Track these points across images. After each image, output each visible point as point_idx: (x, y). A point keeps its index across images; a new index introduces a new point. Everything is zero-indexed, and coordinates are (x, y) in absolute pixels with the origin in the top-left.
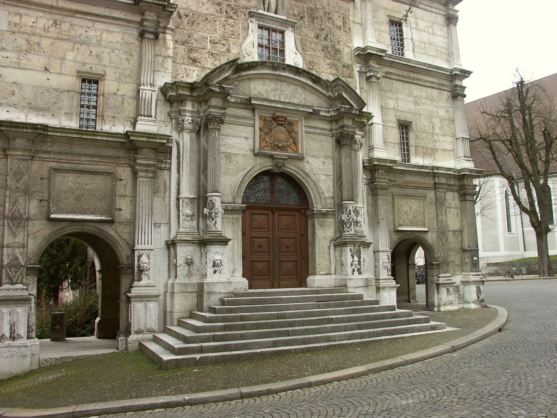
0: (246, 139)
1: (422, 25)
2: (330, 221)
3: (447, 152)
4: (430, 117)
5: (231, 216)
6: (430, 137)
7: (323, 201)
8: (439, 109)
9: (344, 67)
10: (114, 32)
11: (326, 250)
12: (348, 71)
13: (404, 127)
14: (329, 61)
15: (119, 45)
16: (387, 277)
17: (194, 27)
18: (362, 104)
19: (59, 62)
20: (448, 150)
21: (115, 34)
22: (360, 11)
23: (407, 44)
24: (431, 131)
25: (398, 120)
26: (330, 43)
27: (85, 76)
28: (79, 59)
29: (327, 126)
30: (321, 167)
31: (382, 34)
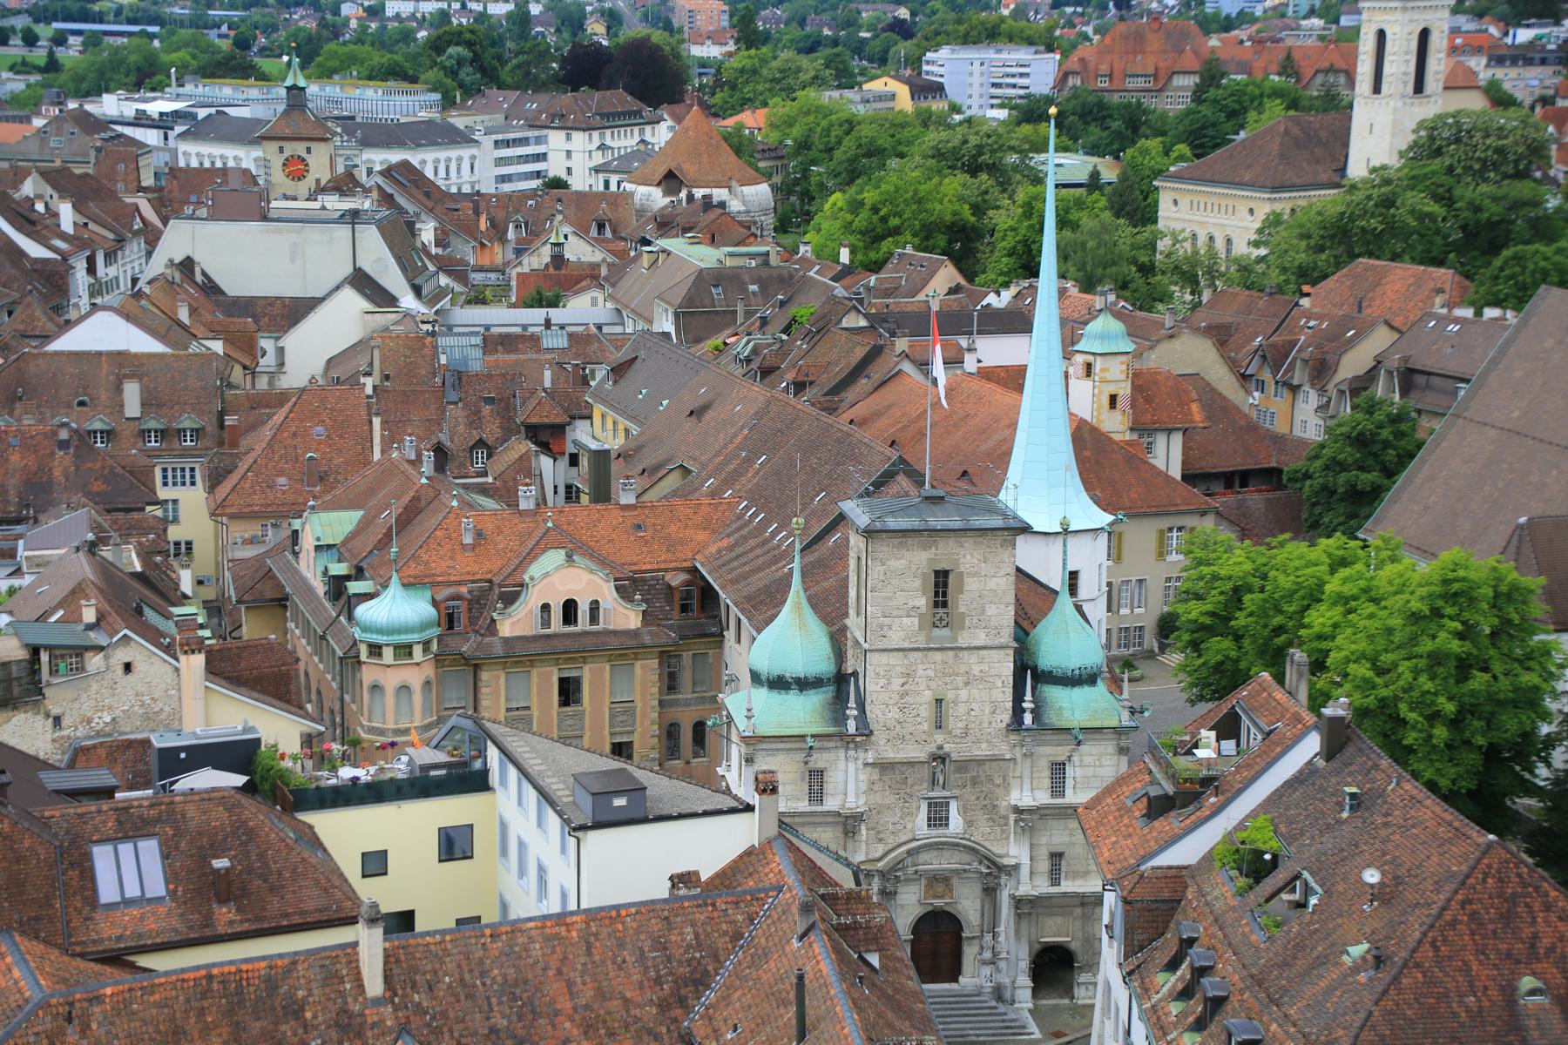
1: (1087, 760)
2: (976, 942)
13: (1056, 857)
23: (1069, 783)
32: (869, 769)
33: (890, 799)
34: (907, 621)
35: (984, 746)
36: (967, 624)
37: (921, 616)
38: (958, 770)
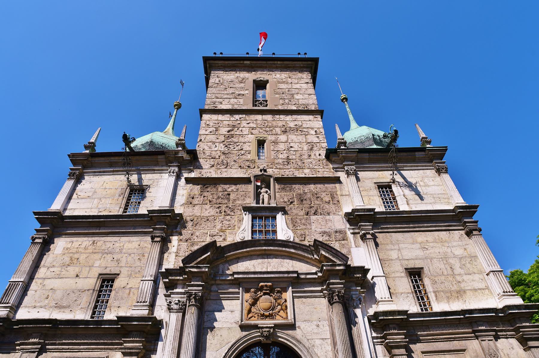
3: (479, 291)
4: (445, 258)
6: (451, 279)
8: (454, 250)
12: (341, 235)
13: (415, 274)
15: (136, 250)
17: (197, 227)
18: (344, 258)
20: (480, 289)
21: (134, 243)
22: (346, 185)
24: (450, 272)
25: (406, 269)
31: (372, 198)
33: (209, 211)
35: (307, 171)
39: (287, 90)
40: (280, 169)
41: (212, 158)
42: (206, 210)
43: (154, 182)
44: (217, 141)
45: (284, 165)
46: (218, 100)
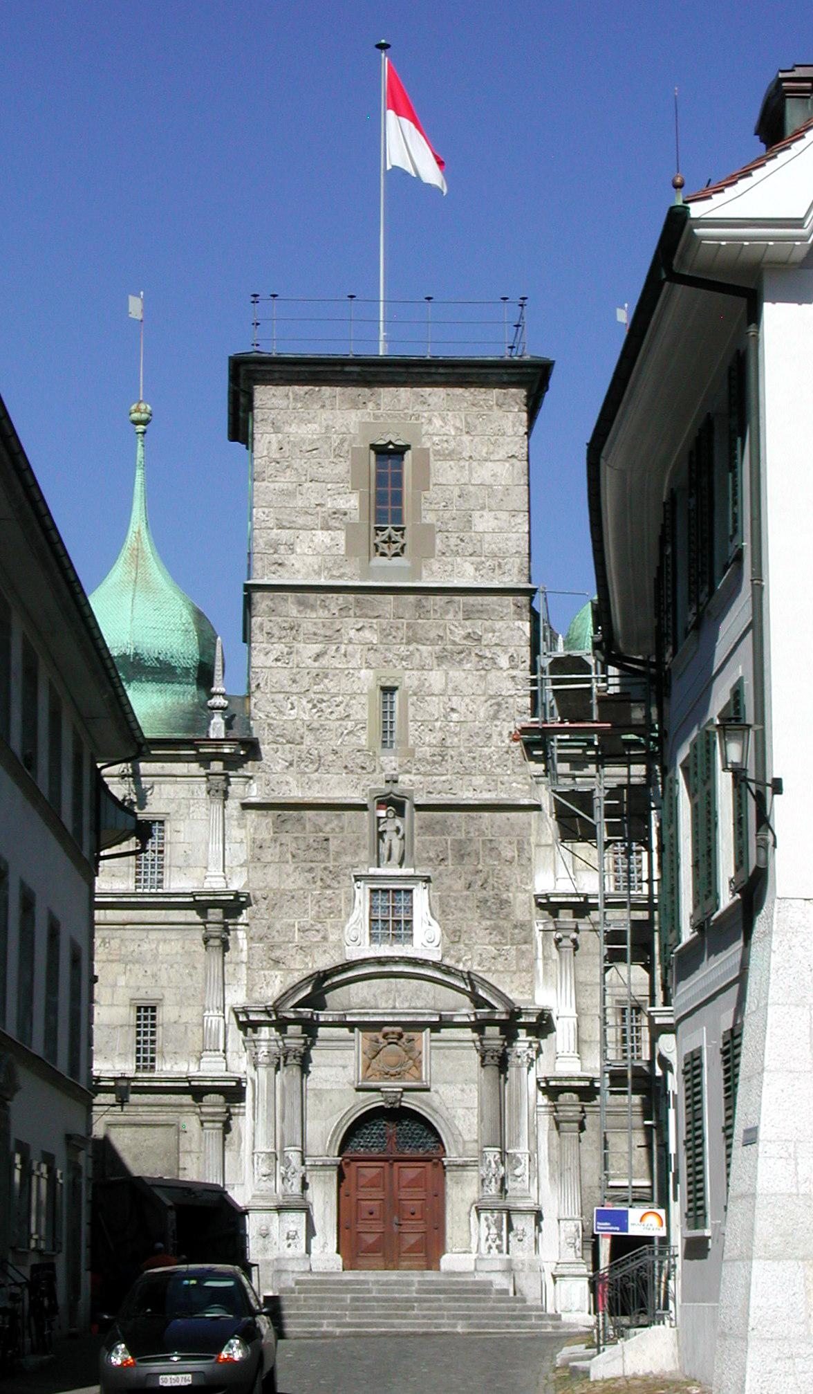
0: (344, 1067)
2: (472, 1175)
5: (321, 1173)
7: (460, 1147)
9: (515, 927)
10: (171, 940)
11: (464, 1217)
12: (523, 933)
14: (488, 923)
16: (573, 1259)
19: (109, 990)
26: (491, 893)
27: (140, 1003)
28: (132, 983)
29: (468, 1034)
30: (459, 1097)
32: (252, 815)
33: (293, 880)
34: (322, 537)
35: (479, 780)
36: (439, 545)
37: (351, 529)
38: (428, 828)
39: (457, 492)
40: (425, 774)
41: (288, 742)
42: (288, 875)
43: (179, 805)
44: (295, 688)
45: (434, 762)
46: (285, 535)
